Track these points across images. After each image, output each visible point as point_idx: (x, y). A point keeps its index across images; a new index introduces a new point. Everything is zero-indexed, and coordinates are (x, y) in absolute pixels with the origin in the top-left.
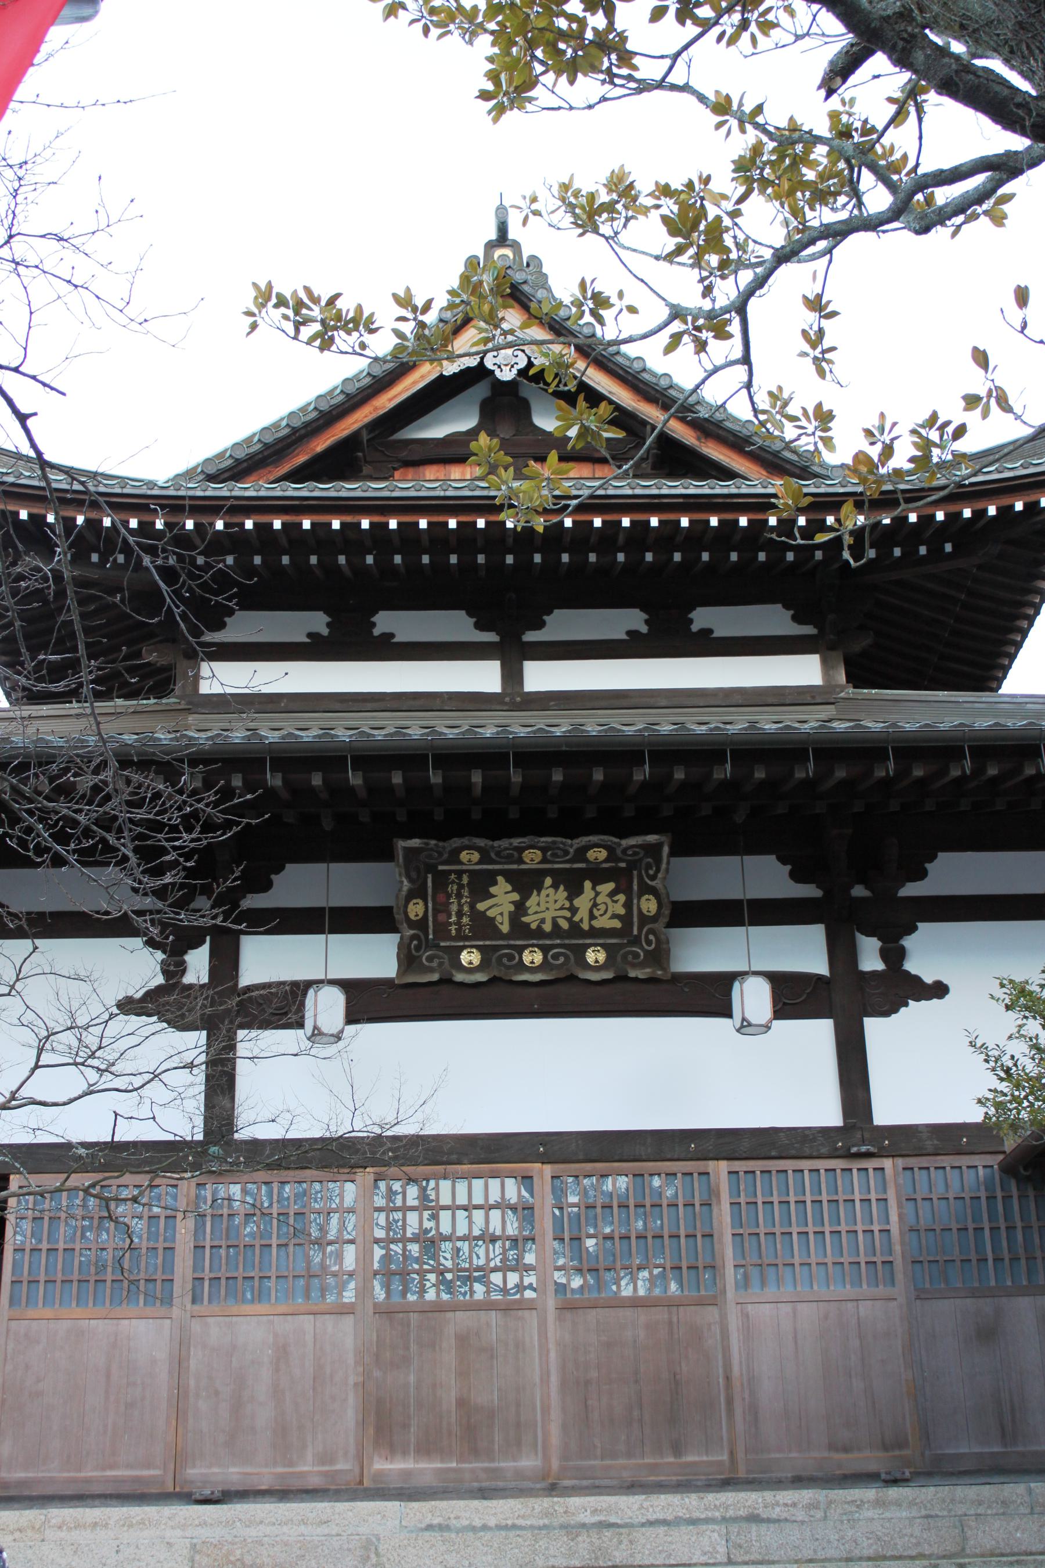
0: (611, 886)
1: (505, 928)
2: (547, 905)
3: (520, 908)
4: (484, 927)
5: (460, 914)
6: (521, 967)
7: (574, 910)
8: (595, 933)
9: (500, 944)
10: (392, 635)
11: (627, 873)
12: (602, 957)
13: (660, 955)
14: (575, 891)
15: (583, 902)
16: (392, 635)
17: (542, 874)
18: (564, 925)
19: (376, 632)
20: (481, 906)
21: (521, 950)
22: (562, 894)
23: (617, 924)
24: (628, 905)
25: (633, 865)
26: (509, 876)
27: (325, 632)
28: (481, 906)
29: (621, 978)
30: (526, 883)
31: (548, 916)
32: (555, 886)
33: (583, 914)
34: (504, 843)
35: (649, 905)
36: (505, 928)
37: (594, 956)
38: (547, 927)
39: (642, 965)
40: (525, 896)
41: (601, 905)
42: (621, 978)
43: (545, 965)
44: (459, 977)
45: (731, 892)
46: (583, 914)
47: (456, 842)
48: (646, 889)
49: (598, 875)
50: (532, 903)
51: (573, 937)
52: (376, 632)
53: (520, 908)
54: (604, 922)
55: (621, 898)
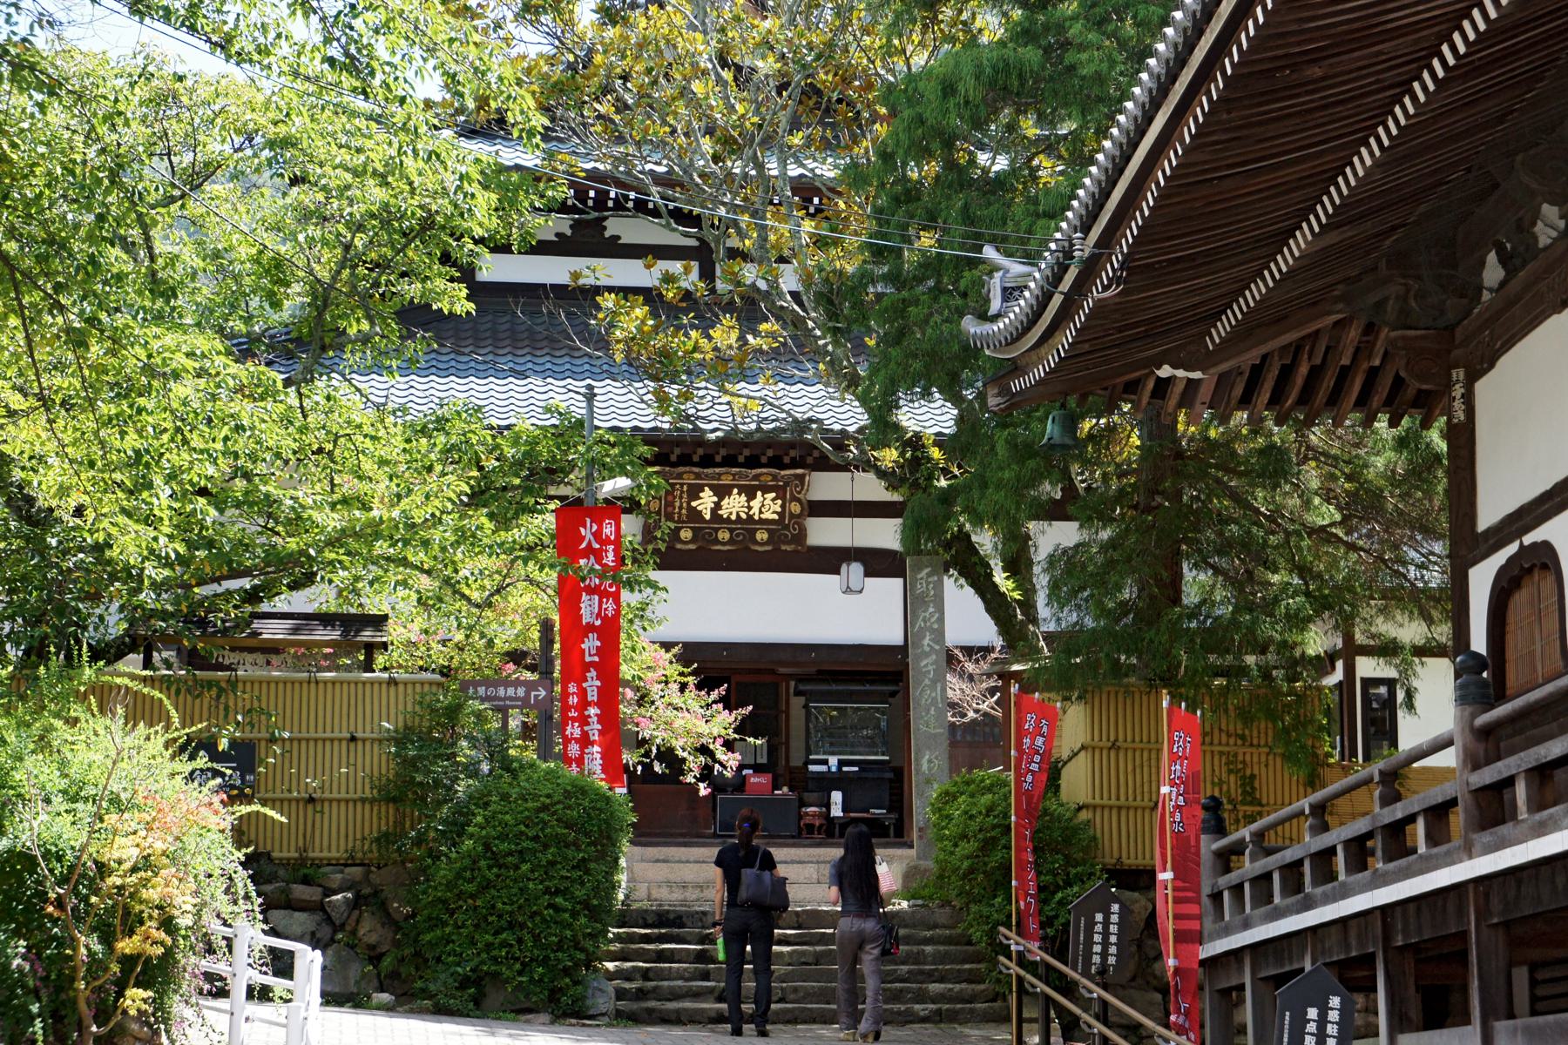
0: (773, 495)
1: (708, 517)
2: (734, 505)
3: (718, 506)
4: (695, 515)
5: (681, 508)
6: (717, 541)
7: (750, 508)
8: (761, 521)
9: (705, 529)
10: (619, 238)
11: (784, 488)
12: (766, 536)
13: (802, 534)
14: (751, 497)
15: (756, 504)
16: (619, 238)
17: (734, 486)
18: (744, 516)
19: (607, 234)
20: (694, 504)
21: (717, 530)
22: (743, 498)
23: (776, 517)
24: (783, 506)
25: (787, 484)
26: (712, 487)
27: (569, 232)
28: (694, 504)
29: (777, 550)
30: (722, 492)
31: (734, 511)
32: (739, 494)
33: (755, 510)
34: (710, 471)
35: (795, 508)
36: (708, 517)
37: (762, 536)
38: (733, 517)
39: (789, 543)
40: (721, 499)
41: (767, 506)
42: (777, 550)
43: (731, 541)
44: (679, 546)
45: (843, 523)
46: (755, 510)
47: (681, 469)
48: (794, 499)
49: (766, 490)
50: (725, 503)
51: (749, 524)
52: (607, 234)
53: (718, 506)
54: (768, 515)
55: (779, 502)
